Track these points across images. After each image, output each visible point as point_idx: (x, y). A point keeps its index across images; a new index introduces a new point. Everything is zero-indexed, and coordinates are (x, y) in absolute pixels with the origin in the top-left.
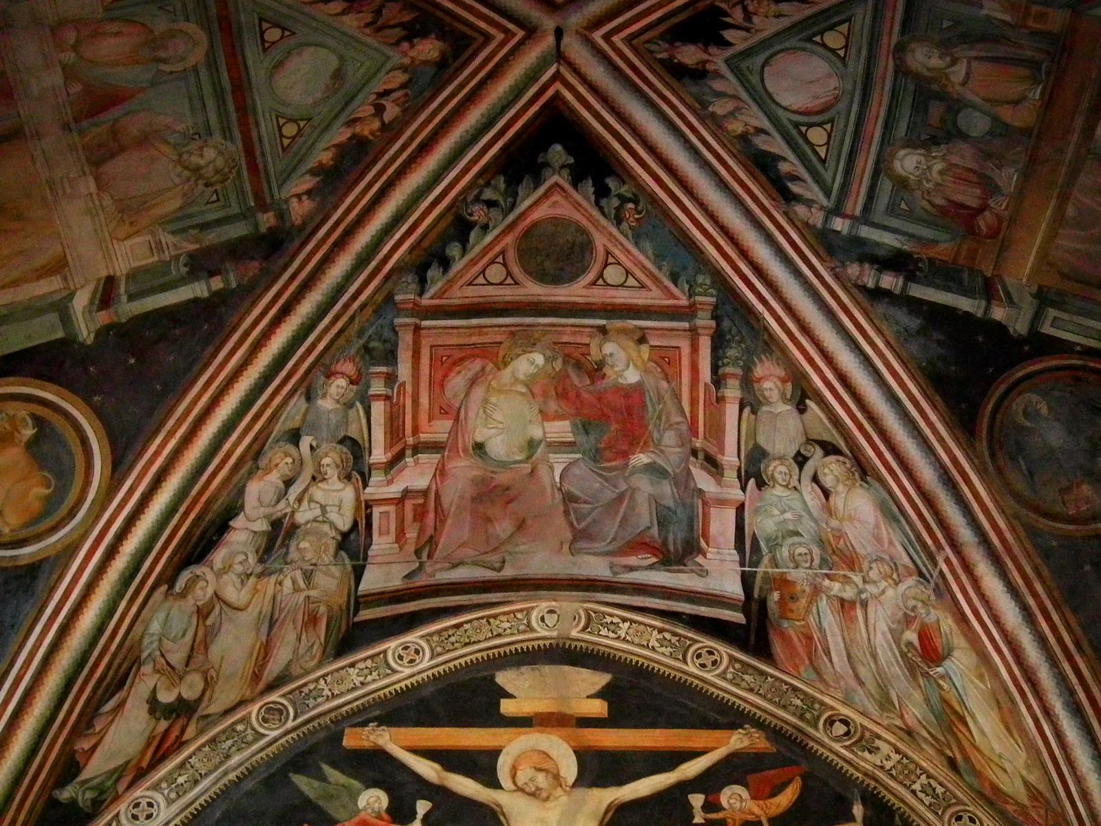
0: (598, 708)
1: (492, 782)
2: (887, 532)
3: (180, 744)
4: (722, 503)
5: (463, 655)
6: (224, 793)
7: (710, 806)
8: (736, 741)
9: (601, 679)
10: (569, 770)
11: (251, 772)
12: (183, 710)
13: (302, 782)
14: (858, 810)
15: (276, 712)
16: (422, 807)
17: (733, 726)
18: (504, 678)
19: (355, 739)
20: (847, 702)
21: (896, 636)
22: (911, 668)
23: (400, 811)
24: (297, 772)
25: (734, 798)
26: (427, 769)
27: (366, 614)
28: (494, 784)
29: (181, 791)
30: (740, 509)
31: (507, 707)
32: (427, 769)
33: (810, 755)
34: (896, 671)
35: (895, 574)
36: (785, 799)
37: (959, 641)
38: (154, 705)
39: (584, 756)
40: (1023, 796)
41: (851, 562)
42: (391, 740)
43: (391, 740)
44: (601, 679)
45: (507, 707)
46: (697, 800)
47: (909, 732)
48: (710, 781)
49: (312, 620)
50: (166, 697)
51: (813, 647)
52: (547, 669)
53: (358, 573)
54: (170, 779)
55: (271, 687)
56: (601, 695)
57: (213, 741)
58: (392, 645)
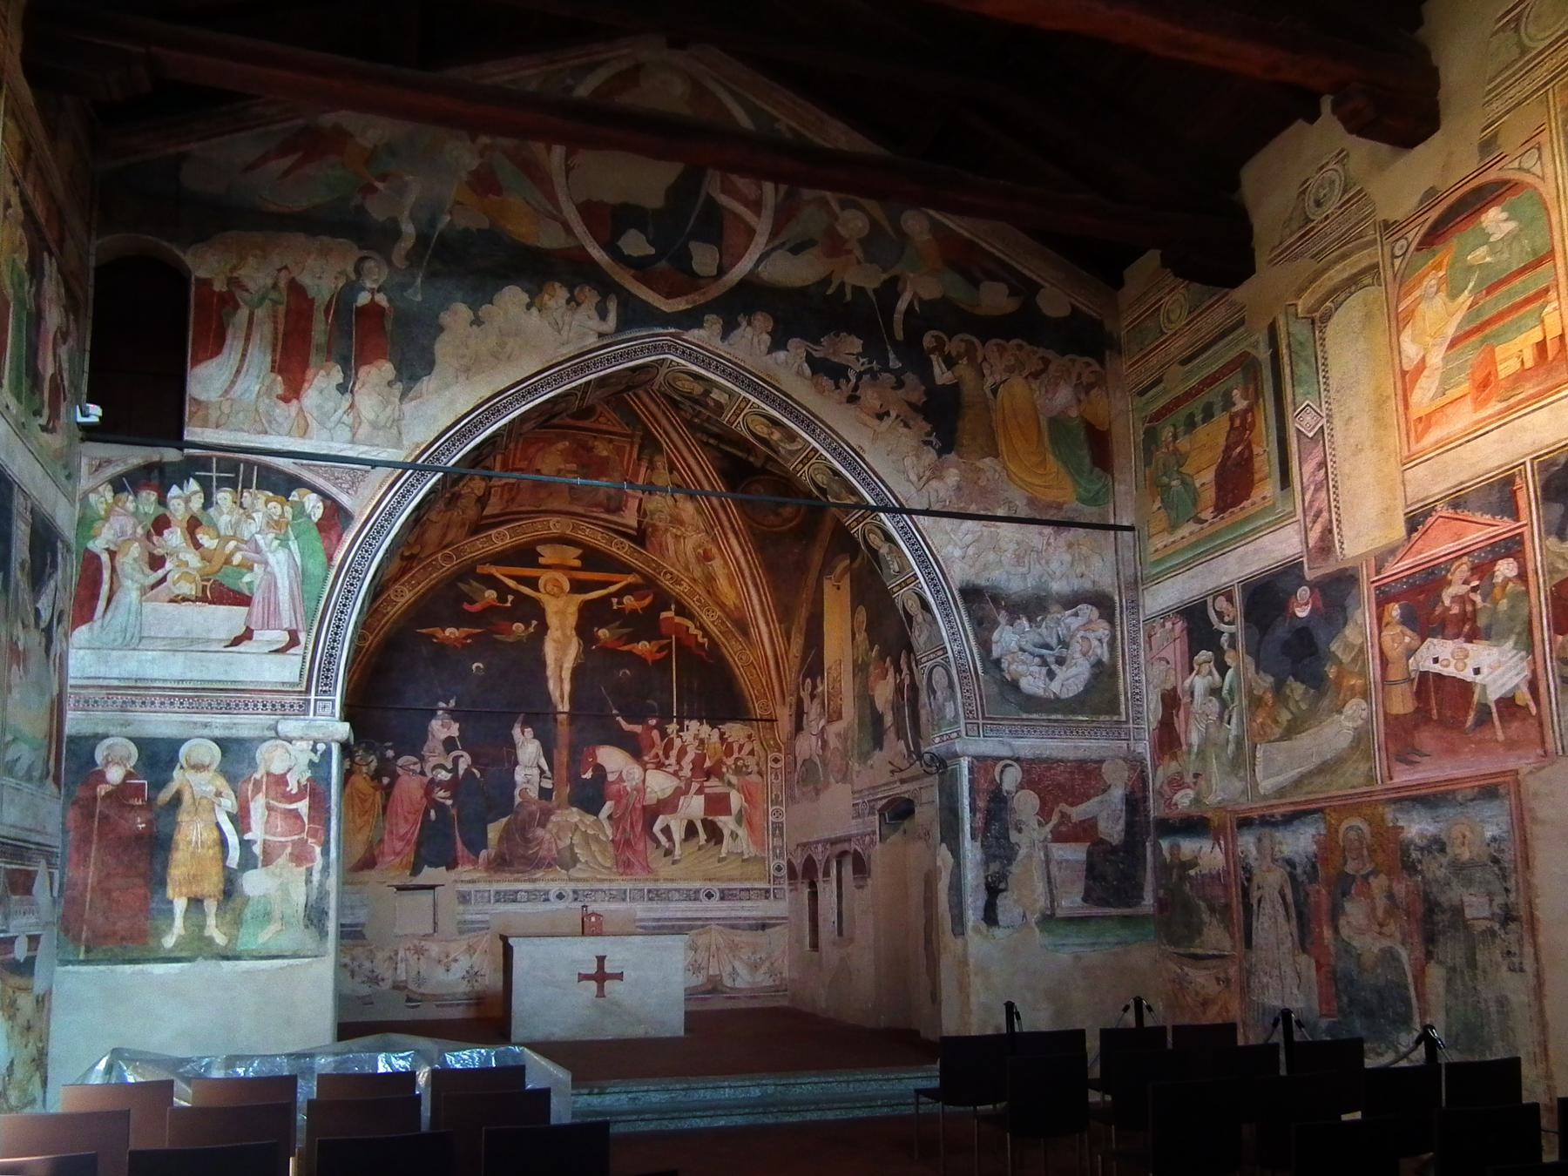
0: (577, 563)
1: (537, 590)
2: (697, 517)
3: (411, 568)
4: (634, 497)
5: (524, 538)
6: (432, 588)
7: (618, 603)
8: (630, 579)
9: (579, 552)
10: (567, 586)
11: (442, 580)
12: (412, 557)
13: (462, 586)
14: (673, 607)
15: (448, 558)
16: (510, 598)
17: (629, 573)
18: (539, 549)
19: (481, 569)
20: (673, 566)
21: (694, 549)
22: (698, 561)
23: (502, 598)
24: (461, 581)
25: (628, 600)
26: (511, 583)
27: (484, 522)
28: (537, 590)
29: (414, 587)
30: (641, 500)
31: (541, 560)
32: (511, 583)
33: (658, 586)
34: (693, 560)
35: (698, 531)
36: (647, 601)
37: (718, 556)
38: (403, 558)
39: (571, 581)
40: (732, 607)
41: (682, 523)
42: (497, 572)
43: (497, 571)
44: (579, 552)
45: (541, 560)
46: (615, 600)
47: (695, 580)
48: (619, 594)
49: (463, 525)
50: (407, 554)
51: (662, 550)
52: (558, 547)
53: (483, 509)
54: (408, 581)
55: (446, 547)
56: (578, 558)
57: (424, 568)
58: (493, 532)
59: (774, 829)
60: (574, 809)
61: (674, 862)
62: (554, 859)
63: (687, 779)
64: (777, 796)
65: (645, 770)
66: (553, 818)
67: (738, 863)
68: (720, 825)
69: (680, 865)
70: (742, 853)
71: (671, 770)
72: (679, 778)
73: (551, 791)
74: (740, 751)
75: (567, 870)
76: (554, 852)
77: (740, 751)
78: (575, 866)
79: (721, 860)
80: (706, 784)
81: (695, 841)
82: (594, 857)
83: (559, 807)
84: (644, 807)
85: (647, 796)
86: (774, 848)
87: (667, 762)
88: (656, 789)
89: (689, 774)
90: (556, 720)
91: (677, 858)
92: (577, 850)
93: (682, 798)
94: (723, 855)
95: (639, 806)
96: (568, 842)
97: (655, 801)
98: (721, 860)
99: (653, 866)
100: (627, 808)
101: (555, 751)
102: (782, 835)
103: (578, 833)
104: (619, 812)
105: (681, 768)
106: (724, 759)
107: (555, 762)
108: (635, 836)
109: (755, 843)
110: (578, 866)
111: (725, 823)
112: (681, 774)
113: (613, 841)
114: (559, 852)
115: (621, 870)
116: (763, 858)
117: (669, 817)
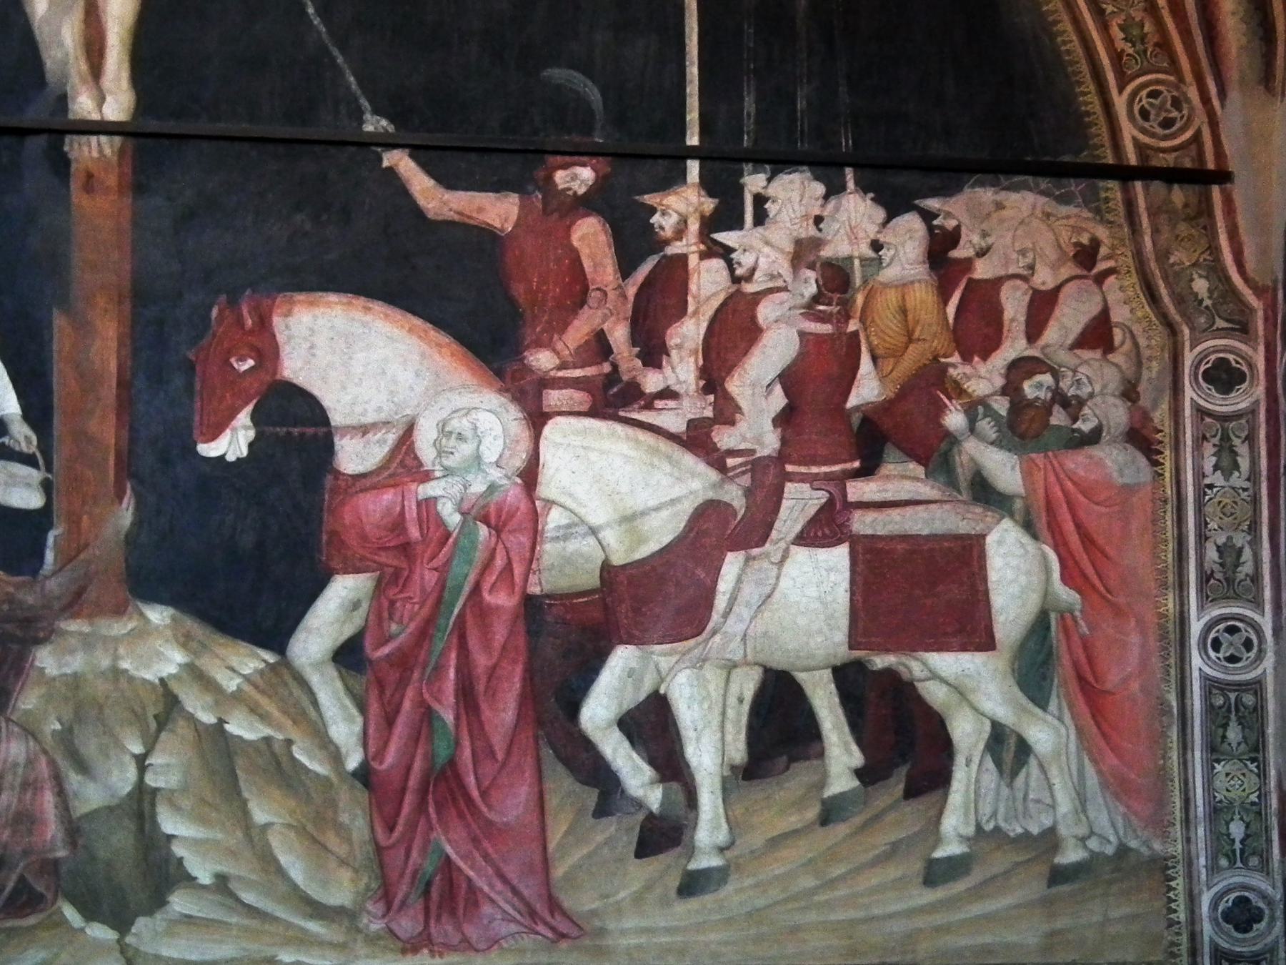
59: (1217, 718)
60: (158, 615)
61: (692, 885)
62: (51, 867)
63: (757, 466)
64: (1229, 553)
65: (537, 419)
66: (46, 660)
67: (1032, 887)
68: (935, 694)
69: (732, 895)
70: (1050, 840)
71: (673, 419)
72: (717, 459)
73: (37, 521)
74: (1034, 330)
75: (122, 924)
76: (52, 829)
77: (1034, 330)
78: (158, 901)
79: (936, 873)
80: (859, 490)
81: (798, 778)
82: (269, 862)
83: (74, 604)
84: (530, 602)
85: (549, 551)
86: (1217, 811)
87: (652, 382)
88: (597, 514)
89: (770, 442)
90: (61, 165)
91: (706, 861)
92: (169, 823)
93: (732, 564)
94: (950, 848)
95: (503, 600)
96: (123, 779)
97: (591, 580)
98: (936, 873)
99: (580, 901)
100: (439, 602)
101: (59, 321)
102: (1256, 749)
103: (181, 726)
104: (401, 632)
105: (727, 412)
106: (957, 369)
107: (62, 380)
108: (484, 752)
109: (1118, 787)
110: (179, 902)
111: (960, 691)
112: (725, 438)
113: (364, 775)
114: (73, 830)
115: (407, 925)
116: (1160, 868)
117: (662, 655)
